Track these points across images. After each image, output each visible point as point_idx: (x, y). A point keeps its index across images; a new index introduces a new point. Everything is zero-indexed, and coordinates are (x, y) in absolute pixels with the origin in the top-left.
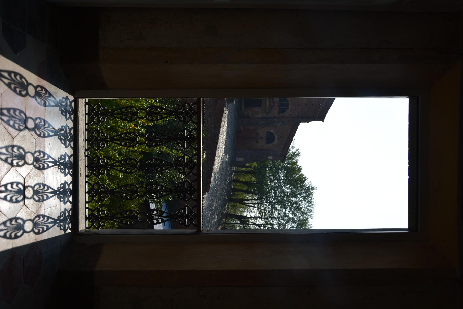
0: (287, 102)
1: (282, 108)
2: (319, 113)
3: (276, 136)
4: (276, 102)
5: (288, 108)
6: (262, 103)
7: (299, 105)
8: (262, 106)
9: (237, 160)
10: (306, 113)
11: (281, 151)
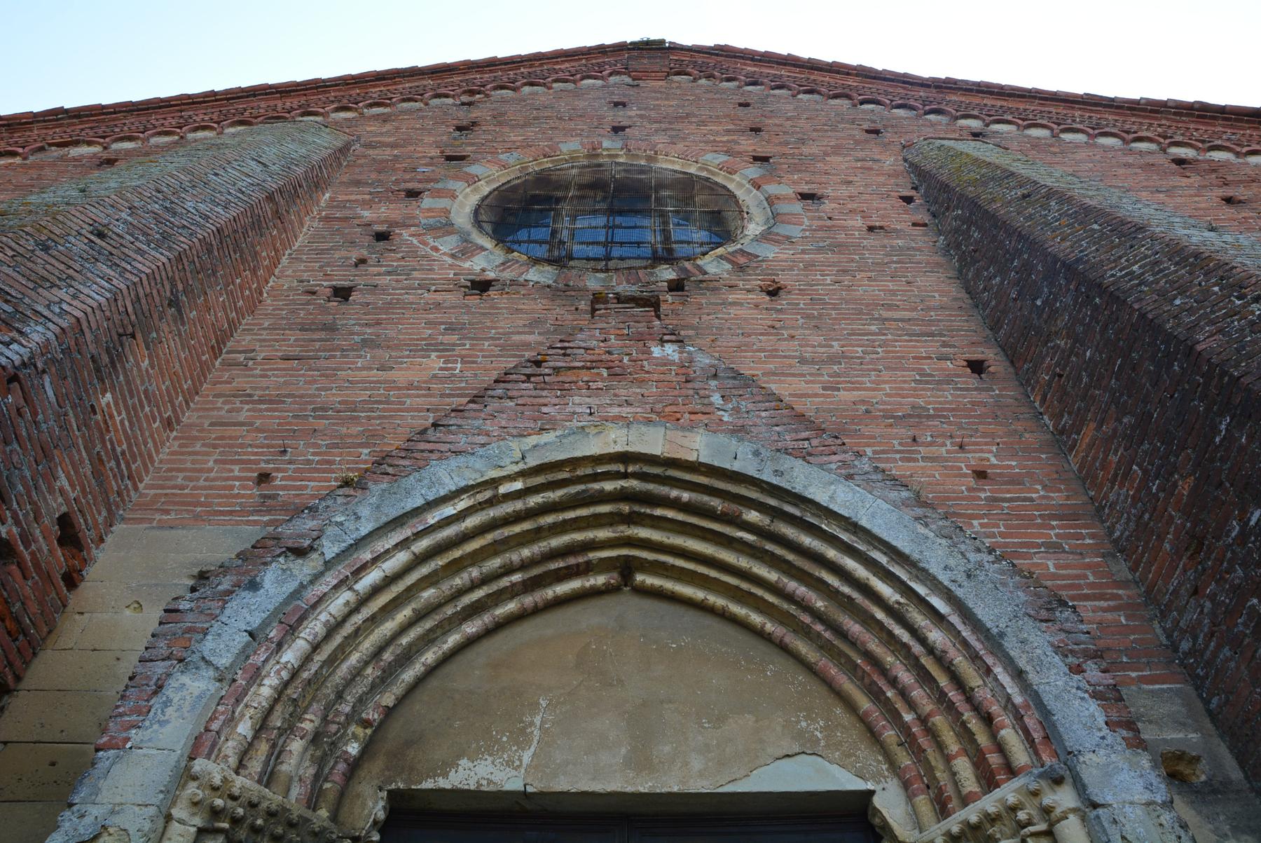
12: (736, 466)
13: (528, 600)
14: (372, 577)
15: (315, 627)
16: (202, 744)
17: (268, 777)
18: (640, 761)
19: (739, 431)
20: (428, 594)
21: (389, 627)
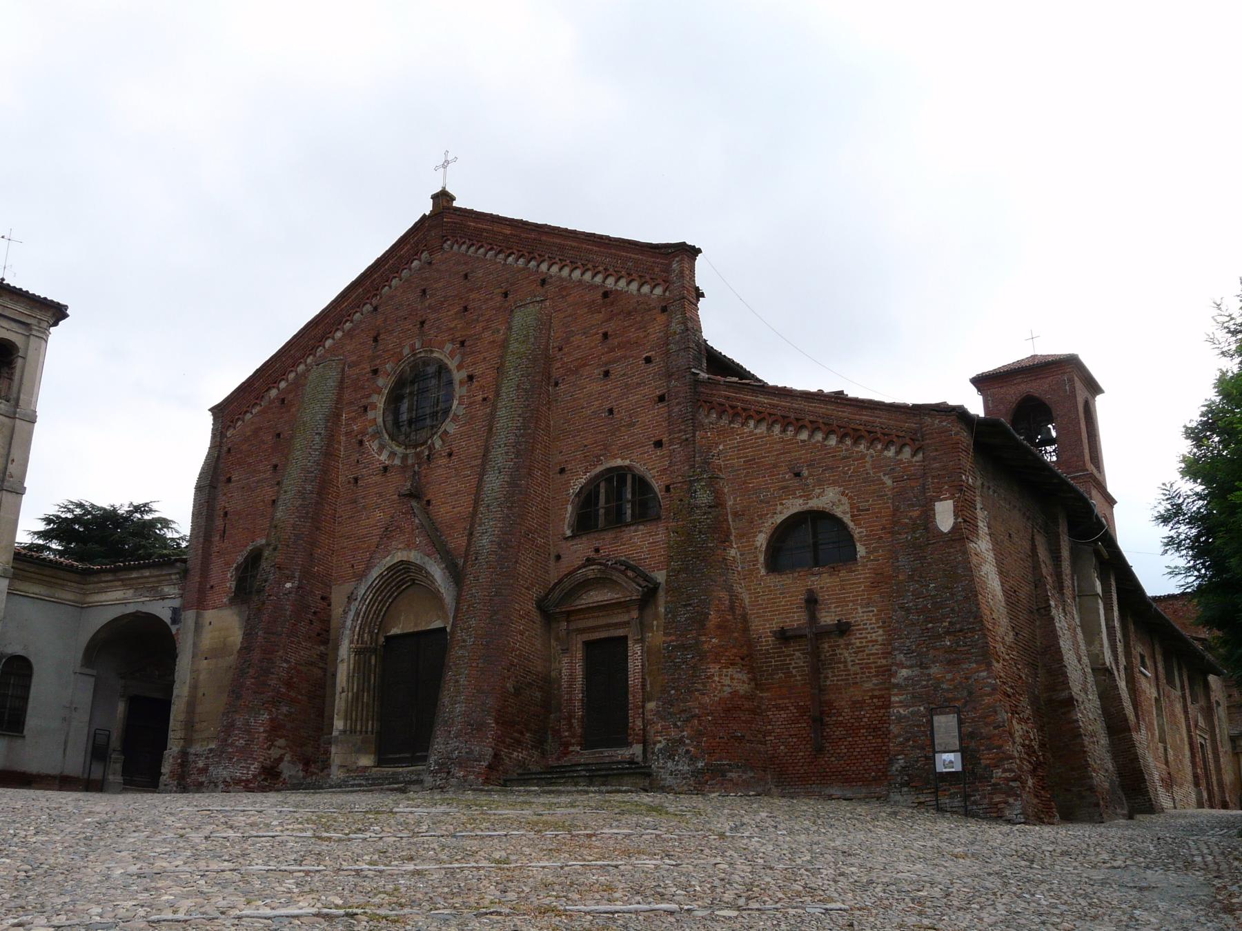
0: (602, 485)
1: (629, 506)
2: (646, 289)
3: (795, 506)
4: (597, 550)
5: (629, 468)
6: (604, 635)
7: (611, 411)
8: (620, 632)
9: (958, 767)
11: (898, 452)
12: (418, 562)
15: (362, 614)
16: (351, 642)
18: (416, 625)
20: (380, 598)
21: (374, 608)
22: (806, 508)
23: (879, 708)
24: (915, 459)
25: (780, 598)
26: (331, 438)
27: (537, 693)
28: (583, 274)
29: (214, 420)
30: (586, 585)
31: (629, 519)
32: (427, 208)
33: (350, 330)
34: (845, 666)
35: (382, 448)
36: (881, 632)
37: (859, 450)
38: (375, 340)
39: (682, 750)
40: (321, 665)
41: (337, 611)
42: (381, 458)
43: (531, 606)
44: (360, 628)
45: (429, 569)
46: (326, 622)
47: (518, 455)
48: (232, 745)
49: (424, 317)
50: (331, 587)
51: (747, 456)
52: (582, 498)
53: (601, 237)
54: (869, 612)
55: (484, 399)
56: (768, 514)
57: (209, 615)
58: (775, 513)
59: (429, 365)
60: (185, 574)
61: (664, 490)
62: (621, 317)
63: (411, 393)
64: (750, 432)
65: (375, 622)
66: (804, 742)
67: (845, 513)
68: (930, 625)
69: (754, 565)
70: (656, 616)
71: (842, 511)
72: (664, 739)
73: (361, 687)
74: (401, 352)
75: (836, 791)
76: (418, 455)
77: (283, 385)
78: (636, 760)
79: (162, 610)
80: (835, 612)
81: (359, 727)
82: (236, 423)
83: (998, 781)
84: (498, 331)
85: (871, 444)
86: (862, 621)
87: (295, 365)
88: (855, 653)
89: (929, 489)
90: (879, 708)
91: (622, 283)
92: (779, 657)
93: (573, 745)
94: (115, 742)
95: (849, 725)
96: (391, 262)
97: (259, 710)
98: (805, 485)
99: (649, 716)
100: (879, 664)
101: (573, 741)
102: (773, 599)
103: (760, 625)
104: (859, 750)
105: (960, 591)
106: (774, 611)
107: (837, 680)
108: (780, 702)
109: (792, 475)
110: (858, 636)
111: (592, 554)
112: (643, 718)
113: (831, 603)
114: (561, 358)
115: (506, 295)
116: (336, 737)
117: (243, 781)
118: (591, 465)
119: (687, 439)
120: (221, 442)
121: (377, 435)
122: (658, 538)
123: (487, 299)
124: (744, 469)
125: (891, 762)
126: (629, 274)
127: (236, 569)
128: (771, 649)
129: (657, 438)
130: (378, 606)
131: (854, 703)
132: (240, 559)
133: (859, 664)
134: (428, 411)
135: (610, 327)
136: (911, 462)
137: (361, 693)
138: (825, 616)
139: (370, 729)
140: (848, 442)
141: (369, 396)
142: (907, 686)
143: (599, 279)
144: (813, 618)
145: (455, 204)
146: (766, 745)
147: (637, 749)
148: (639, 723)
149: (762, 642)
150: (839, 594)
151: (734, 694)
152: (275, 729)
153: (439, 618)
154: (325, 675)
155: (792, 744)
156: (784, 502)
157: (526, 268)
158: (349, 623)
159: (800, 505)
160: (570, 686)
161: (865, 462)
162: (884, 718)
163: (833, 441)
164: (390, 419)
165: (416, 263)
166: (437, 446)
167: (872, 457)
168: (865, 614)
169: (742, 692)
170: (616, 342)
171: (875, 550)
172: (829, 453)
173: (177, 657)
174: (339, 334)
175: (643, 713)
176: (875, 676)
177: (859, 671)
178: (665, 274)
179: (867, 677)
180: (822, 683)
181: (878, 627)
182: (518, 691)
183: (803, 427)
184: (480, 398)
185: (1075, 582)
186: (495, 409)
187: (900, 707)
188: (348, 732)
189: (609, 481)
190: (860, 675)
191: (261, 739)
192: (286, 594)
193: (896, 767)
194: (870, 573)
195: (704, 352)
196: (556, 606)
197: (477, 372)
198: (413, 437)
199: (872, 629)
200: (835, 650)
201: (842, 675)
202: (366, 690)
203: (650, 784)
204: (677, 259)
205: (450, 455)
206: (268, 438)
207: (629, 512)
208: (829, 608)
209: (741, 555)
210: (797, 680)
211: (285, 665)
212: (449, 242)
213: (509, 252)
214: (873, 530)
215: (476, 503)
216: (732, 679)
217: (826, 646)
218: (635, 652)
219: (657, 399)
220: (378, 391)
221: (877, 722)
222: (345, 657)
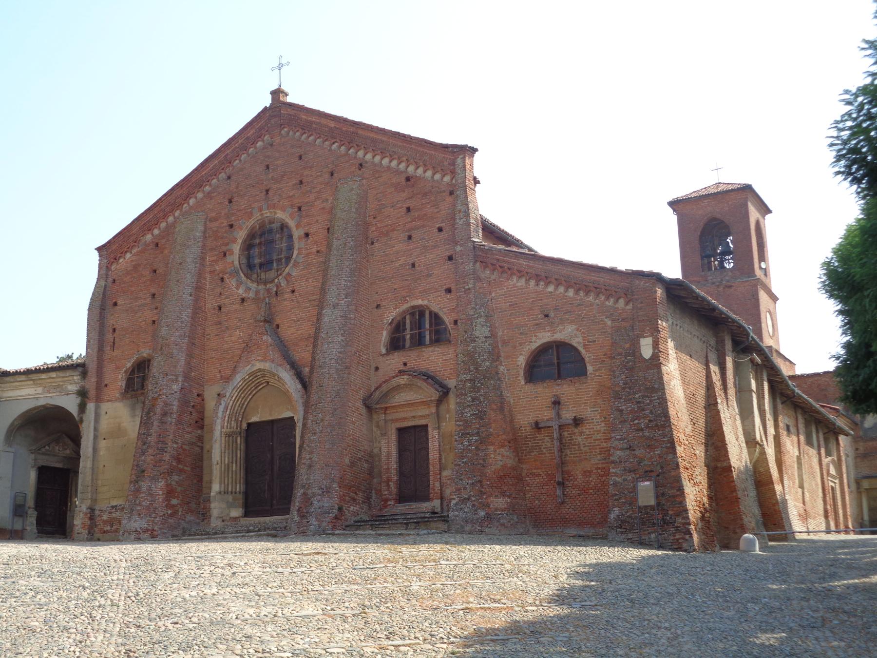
0: (408, 317)
1: (427, 333)
2: (437, 177)
3: (544, 337)
4: (405, 364)
10: (440, 230)
13: (257, 390)
14: (234, 398)
15: (229, 407)
16: (222, 427)
17: (230, 428)
19: (273, 361)
20: (242, 395)
22: (552, 339)
23: (600, 475)
24: (628, 307)
25: (534, 400)
26: (200, 275)
27: (364, 464)
28: (390, 162)
29: (100, 256)
30: (398, 388)
31: (427, 342)
32: (267, 101)
33: (209, 193)
34: (579, 447)
35: (239, 284)
36: (603, 425)
37: (589, 300)
38: (230, 202)
39: (469, 504)
40: (199, 444)
41: (210, 403)
42: (239, 292)
43: (359, 404)
44: (229, 417)
45: (281, 375)
46: (201, 413)
47: (347, 296)
48: (140, 505)
49: (268, 187)
50: (203, 386)
51: (511, 302)
52: (393, 325)
53: (404, 136)
54: (595, 411)
55: (318, 252)
56: (526, 342)
57: (105, 406)
58: (531, 342)
59: (273, 223)
60: (84, 375)
61: (453, 323)
62: (420, 196)
63: (260, 244)
64: (514, 285)
65: (239, 413)
66: (551, 499)
67: (578, 343)
68: (636, 422)
69: (516, 377)
70: (448, 411)
71: (577, 342)
72: (458, 497)
73: (231, 461)
74: (251, 213)
75: (573, 531)
76: (268, 291)
77: (156, 232)
78: (436, 510)
79: (70, 404)
80: (573, 410)
81: (230, 489)
82: (119, 260)
83: (679, 525)
84: (327, 200)
85: (598, 295)
86: (590, 417)
87: (165, 217)
88: (585, 438)
89: (636, 329)
90: (603, 475)
91: (420, 171)
92: (535, 440)
93: (390, 500)
94: (31, 502)
95: (581, 487)
96: (240, 142)
97: (158, 479)
98: (552, 322)
99: (444, 480)
100: (602, 446)
101: (390, 497)
102: (530, 401)
103: (522, 419)
104: (588, 503)
105: (656, 400)
106: (529, 409)
107: (574, 457)
108: (535, 471)
109: (543, 316)
110: (588, 427)
111: (402, 368)
112: (440, 481)
113: (569, 405)
114: (376, 224)
115: (332, 174)
116: (215, 497)
117: (148, 530)
118: (400, 303)
119: (469, 289)
120: (107, 275)
121: (234, 274)
122: (449, 357)
123: (317, 176)
124: (509, 311)
125: (610, 512)
126: (425, 165)
127: (125, 372)
128: (529, 435)
129: (447, 286)
130: (241, 401)
131: (585, 472)
132: (129, 365)
133: (588, 446)
134: (275, 257)
135: (411, 203)
136: (625, 309)
137: (230, 465)
138: (566, 413)
139: (238, 490)
140: (582, 293)
141: (227, 244)
142: (621, 462)
143: (402, 166)
144: (559, 416)
145: (289, 99)
146: (525, 500)
147: (436, 503)
148: (437, 485)
149: (522, 430)
150: (575, 399)
151: (504, 466)
152: (170, 492)
153: (288, 410)
154: (202, 452)
155: (543, 499)
156: (537, 334)
157: (347, 154)
158: (220, 415)
159: (548, 337)
160: (388, 459)
161: (593, 309)
162: (605, 482)
163: (571, 293)
164: (244, 261)
165: (260, 144)
166: (282, 285)
167: (598, 305)
168: (593, 413)
169: (509, 465)
170: (416, 214)
171: (599, 369)
172: (569, 301)
173: (81, 438)
174: (200, 195)
175: (440, 479)
176: (598, 454)
177: (588, 451)
178: (452, 167)
179: (594, 455)
180: (563, 459)
181: (601, 422)
182: (353, 464)
183: (549, 282)
184: (314, 250)
185: (737, 381)
186: (326, 262)
187: (617, 475)
188: (223, 493)
189: (413, 314)
190: (589, 454)
191: (160, 500)
192: (173, 394)
193: (612, 516)
194: (596, 385)
195: (480, 224)
196: (377, 403)
197: (311, 231)
198: (263, 276)
199: (597, 422)
200: (572, 437)
201: (577, 454)
202: (234, 462)
203: (448, 527)
204: (461, 156)
205: (293, 291)
206: (146, 273)
207: (427, 338)
208: (568, 408)
209: (507, 370)
210: (546, 457)
211: (175, 446)
212: (286, 129)
213: (335, 140)
214: (598, 356)
215: (318, 329)
216: (503, 456)
217: (566, 433)
218: (433, 435)
219: (447, 258)
220: (234, 241)
221: (600, 485)
222: (219, 439)
